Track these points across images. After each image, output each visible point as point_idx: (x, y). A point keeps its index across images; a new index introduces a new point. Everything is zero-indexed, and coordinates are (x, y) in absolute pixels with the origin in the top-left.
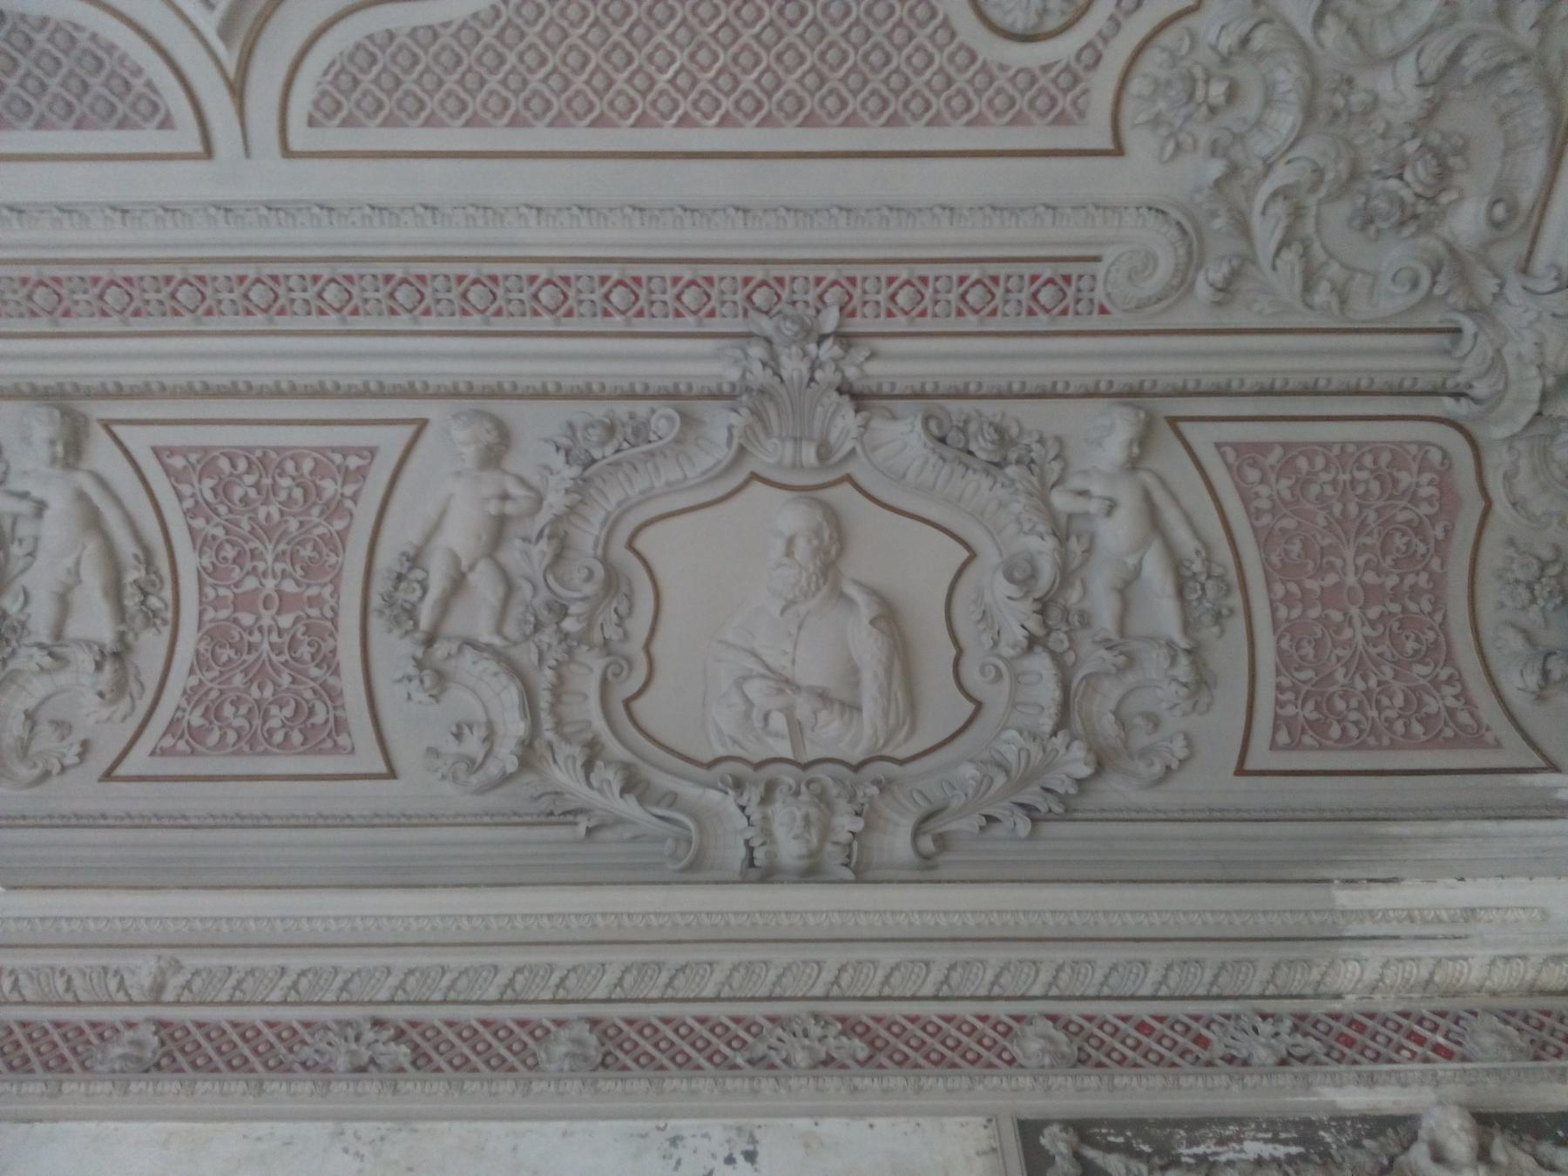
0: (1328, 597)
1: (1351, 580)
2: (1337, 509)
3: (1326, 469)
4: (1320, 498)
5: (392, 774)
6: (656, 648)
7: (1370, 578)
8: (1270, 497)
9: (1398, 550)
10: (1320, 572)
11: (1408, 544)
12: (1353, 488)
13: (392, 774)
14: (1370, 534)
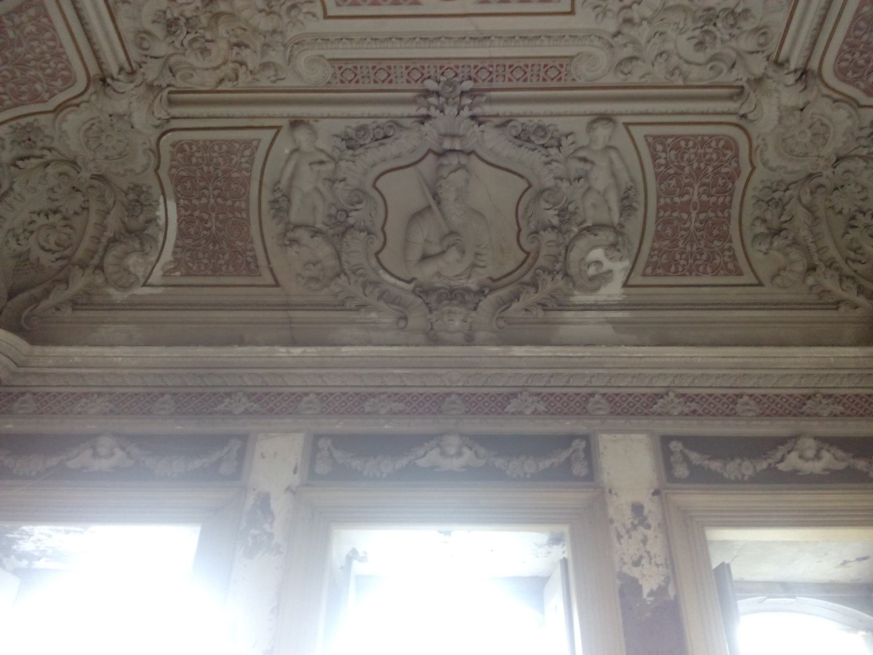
0: (685, 207)
1: (695, 198)
2: (695, 165)
3: (694, 147)
4: (689, 161)
5: (277, 284)
6: (387, 228)
7: (704, 198)
8: (666, 158)
9: (719, 185)
10: (681, 195)
11: (725, 184)
12: (705, 157)
13: (277, 284)
14: (708, 178)
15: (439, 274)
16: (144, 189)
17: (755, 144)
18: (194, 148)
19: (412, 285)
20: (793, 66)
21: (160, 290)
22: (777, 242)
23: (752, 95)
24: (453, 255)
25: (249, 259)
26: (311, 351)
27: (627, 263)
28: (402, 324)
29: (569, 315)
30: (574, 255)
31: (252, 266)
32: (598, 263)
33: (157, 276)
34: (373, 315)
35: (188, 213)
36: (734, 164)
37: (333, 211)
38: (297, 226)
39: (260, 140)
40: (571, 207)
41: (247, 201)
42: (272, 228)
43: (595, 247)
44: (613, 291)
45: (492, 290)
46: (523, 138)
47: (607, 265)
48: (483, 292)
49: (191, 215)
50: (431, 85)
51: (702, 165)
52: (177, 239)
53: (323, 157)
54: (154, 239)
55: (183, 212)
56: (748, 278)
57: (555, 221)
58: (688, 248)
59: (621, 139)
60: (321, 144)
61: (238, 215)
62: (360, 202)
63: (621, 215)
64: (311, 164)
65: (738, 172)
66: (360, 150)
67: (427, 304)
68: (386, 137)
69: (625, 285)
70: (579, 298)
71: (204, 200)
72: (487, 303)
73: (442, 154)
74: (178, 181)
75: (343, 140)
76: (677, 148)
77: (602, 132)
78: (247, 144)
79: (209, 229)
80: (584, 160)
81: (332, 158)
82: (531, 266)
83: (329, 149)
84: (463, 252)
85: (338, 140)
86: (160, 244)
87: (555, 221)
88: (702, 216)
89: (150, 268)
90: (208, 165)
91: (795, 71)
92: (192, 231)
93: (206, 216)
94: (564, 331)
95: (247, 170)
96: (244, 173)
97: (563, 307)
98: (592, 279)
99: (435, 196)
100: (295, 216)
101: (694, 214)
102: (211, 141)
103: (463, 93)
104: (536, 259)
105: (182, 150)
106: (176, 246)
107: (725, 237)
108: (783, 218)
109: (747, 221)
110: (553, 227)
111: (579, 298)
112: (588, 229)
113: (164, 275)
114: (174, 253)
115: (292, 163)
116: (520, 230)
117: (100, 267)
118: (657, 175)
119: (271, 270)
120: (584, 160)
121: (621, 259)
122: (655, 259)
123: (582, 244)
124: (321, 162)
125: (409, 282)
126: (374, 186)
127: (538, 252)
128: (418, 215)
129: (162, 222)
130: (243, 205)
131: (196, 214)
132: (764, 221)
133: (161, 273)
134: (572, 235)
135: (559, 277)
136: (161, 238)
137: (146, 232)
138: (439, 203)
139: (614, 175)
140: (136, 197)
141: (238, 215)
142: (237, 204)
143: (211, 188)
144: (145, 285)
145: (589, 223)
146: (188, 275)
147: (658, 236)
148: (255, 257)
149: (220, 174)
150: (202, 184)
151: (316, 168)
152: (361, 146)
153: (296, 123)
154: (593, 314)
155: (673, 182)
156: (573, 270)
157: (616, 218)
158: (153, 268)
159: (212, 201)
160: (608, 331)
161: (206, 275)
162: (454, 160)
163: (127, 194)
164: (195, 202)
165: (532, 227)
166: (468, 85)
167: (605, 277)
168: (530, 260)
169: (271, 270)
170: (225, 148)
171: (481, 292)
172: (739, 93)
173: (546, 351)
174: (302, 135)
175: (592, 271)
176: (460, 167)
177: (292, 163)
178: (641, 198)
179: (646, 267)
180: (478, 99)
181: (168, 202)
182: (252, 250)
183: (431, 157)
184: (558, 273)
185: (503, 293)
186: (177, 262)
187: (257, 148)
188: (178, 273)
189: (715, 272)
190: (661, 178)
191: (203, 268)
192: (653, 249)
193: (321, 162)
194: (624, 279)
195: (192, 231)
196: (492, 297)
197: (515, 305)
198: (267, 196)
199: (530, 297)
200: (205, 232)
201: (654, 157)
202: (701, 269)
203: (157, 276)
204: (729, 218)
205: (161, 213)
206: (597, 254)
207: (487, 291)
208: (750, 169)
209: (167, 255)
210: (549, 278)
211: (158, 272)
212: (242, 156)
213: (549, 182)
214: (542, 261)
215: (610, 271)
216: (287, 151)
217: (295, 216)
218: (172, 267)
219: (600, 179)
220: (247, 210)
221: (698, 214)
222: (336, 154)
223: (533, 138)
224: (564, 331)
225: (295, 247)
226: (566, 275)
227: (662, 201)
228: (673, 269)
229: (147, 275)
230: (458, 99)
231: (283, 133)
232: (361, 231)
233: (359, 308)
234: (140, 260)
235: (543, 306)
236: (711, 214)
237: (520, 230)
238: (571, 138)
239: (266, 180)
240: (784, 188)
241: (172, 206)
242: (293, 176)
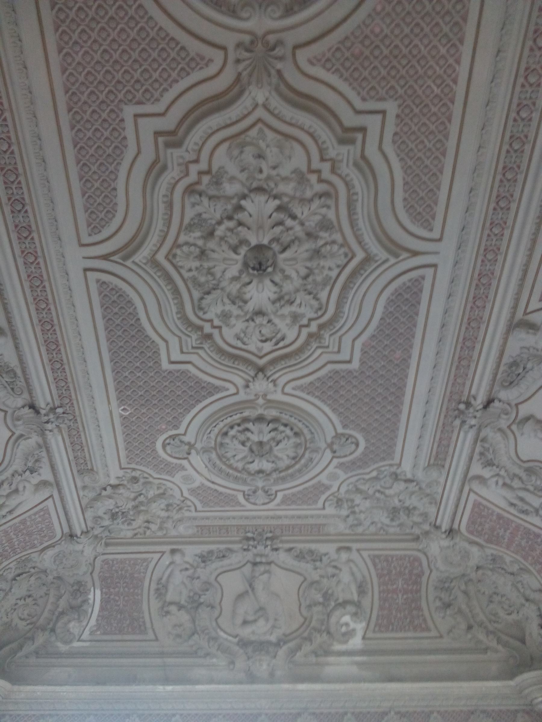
2: (398, 569)
7: (405, 586)
13: (157, 639)
15: (253, 633)
16: (83, 583)
17: (430, 560)
18: (115, 562)
19: (237, 639)
20: (443, 529)
21: (87, 644)
22: (448, 612)
23: (424, 540)
24: (261, 622)
25: (141, 623)
26: (178, 688)
27: (364, 624)
28: (232, 667)
29: (331, 659)
30: (333, 620)
31: (143, 628)
32: (347, 624)
33: (86, 635)
34: (214, 660)
35: (108, 596)
36: (420, 569)
37: (192, 594)
38: (171, 603)
39: (153, 558)
40: (330, 592)
41: (142, 591)
42: (155, 604)
43: (344, 615)
44: (356, 642)
45: (285, 643)
46: (300, 556)
47: (352, 625)
48: (279, 645)
49: (109, 598)
50: (250, 535)
51: (403, 569)
52: (99, 611)
53: (188, 566)
54: (86, 612)
55: (104, 596)
56: (434, 633)
57: (321, 600)
58: (399, 615)
59: (354, 555)
60: (188, 559)
61: (137, 598)
62: (207, 590)
63: (359, 596)
64: (181, 571)
65: (423, 573)
66: (209, 563)
67: (246, 654)
68: (224, 556)
69: (364, 638)
70: (338, 647)
71: (117, 590)
72: (282, 652)
73: (255, 564)
74: (103, 579)
75: (199, 557)
76: (387, 560)
77: (344, 556)
78: (145, 560)
79: (119, 606)
80: (335, 567)
81: (192, 566)
82: (308, 626)
83: (191, 561)
84: (267, 620)
85: (197, 558)
86: (89, 615)
87: (321, 600)
88: (405, 596)
89: (82, 629)
90: (121, 570)
91: (445, 532)
92: (109, 607)
93: (117, 598)
94: (328, 670)
95: (143, 573)
96: (142, 574)
97: (327, 653)
98: (344, 634)
99: (251, 585)
100: (169, 597)
101: (400, 596)
102: (125, 559)
103: (267, 538)
104: (310, 622)
105: (107, 563)
106: (99, 616)
107: (419, 608)
108: (452, 598)
109: (431, 598)
110: (320, 603)
111: (338, 647)
112: (340, 604)
113: (90, 634)
114: (97, 620)
115: (169, 570)
116: (300, 605)
117: (53, 630)
118: (377, 575)
119: (154, 630)
120: (335, 567)
121: (361, 622)
122: (380, 621)
123: (337, 613)
124: (187, 569)
125: (236, 637)
126: (216, 579)
127: (312, 617)
128: (241, 596)
129: (91, 602)
130: (140, 591)
131: (112, 597)
132: (441, 599)
133: (89, 633)
134: (331, 607)
135: (324, 634)
136: (90, 610)
137: (82, 608)
138: (253, 589)
139: (353, 574)
140: (78, 588)
141: (137, 598)
142: (136, 591)
143: (122, 582)
144: (79, 640)
145: (341, 600)
146: (104, 634)
147: (381, 608)
148: (144, 622)
149: (128, 575)
150: (117, 580)
151: (183, 573)
152: (210, 560)
153: (173, 552)
154: (344, 659)
155: (387, 578)
156: (333, 629)
157: (356, 597)
158: (84, 629)
159: (122, 590)
160: (354, 670)
161: (115, 634)
162: (262, 568)
163: (72, 586)
164: (112, 590)
165: (308, 602)
166: (269, 535)
167: (350, 634)
168: (307, 623)
169: (154, 630)
170: (132, 562)
171: (278, 644)
172: (417, 539)
173: (318, 687)
174: (177, 558)
175: (344, 629)
176: (265, 572)
177: (169, 570)
178: (369, 586)
179: (375, 626)
180: (275, 541)
181: (96, 591)
182: (143, 617)
183: (249, 566)
184: (324, 631)
185: (291, 645)
186: (98, 626)
187: (150, 562)
188: (99, 633)
189: (415, 629)
190: (380, 576)
191: (113, 629)
192: (378, 616)
193: (187, 569)
194: (363, 634)
195: (109, 607)
196: (285, 648)
197: (298, 654)
198: (154, 586)
199: (307, 648)
200: (116, 608)
201: (375, 565)
202: (407, 628)
203: (86, 635)
204: (420, 597)
205: (91, 596)
206: (346, 619)
207: (282, 644)
208: (429, 572)
209: (93, 622)
210: (318, 636)
211: (87, 632)
212: (142, 566)
213: (316, 578)
214: (314, 623)
215: (354, 630)
216: (167, 563)
217: (169, 597)
218: (95, 629)
219: (345, 577)
220: (142, 595)
221: (403, 595)
222: (195, 564)
223: (306, 556)
224: (328, 670)
225: (168, 617)
226: (329, 633)
227: (382, 588)
228: (391, 628)
229: (80, 634)
230: (264, 542)
231: (165, 556)
232: (208, 606)
233: (207, 655)
234: (77, 625)
235: (315, 654)
236: (410, 595)
237: (300, 605)
238: (327, 557)
239: (155, 578)
240: (450, 581)
241: (98, 592)
242: (169, 576)
